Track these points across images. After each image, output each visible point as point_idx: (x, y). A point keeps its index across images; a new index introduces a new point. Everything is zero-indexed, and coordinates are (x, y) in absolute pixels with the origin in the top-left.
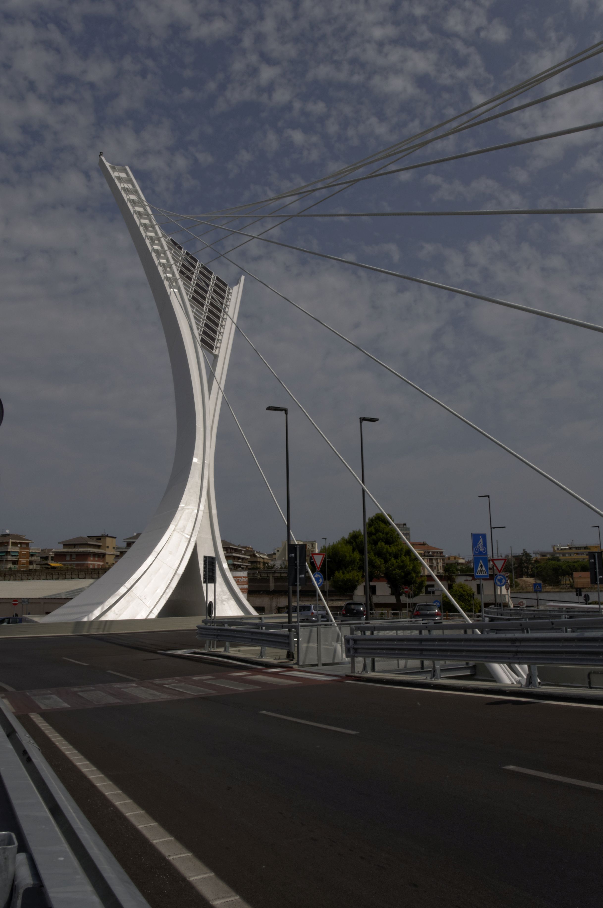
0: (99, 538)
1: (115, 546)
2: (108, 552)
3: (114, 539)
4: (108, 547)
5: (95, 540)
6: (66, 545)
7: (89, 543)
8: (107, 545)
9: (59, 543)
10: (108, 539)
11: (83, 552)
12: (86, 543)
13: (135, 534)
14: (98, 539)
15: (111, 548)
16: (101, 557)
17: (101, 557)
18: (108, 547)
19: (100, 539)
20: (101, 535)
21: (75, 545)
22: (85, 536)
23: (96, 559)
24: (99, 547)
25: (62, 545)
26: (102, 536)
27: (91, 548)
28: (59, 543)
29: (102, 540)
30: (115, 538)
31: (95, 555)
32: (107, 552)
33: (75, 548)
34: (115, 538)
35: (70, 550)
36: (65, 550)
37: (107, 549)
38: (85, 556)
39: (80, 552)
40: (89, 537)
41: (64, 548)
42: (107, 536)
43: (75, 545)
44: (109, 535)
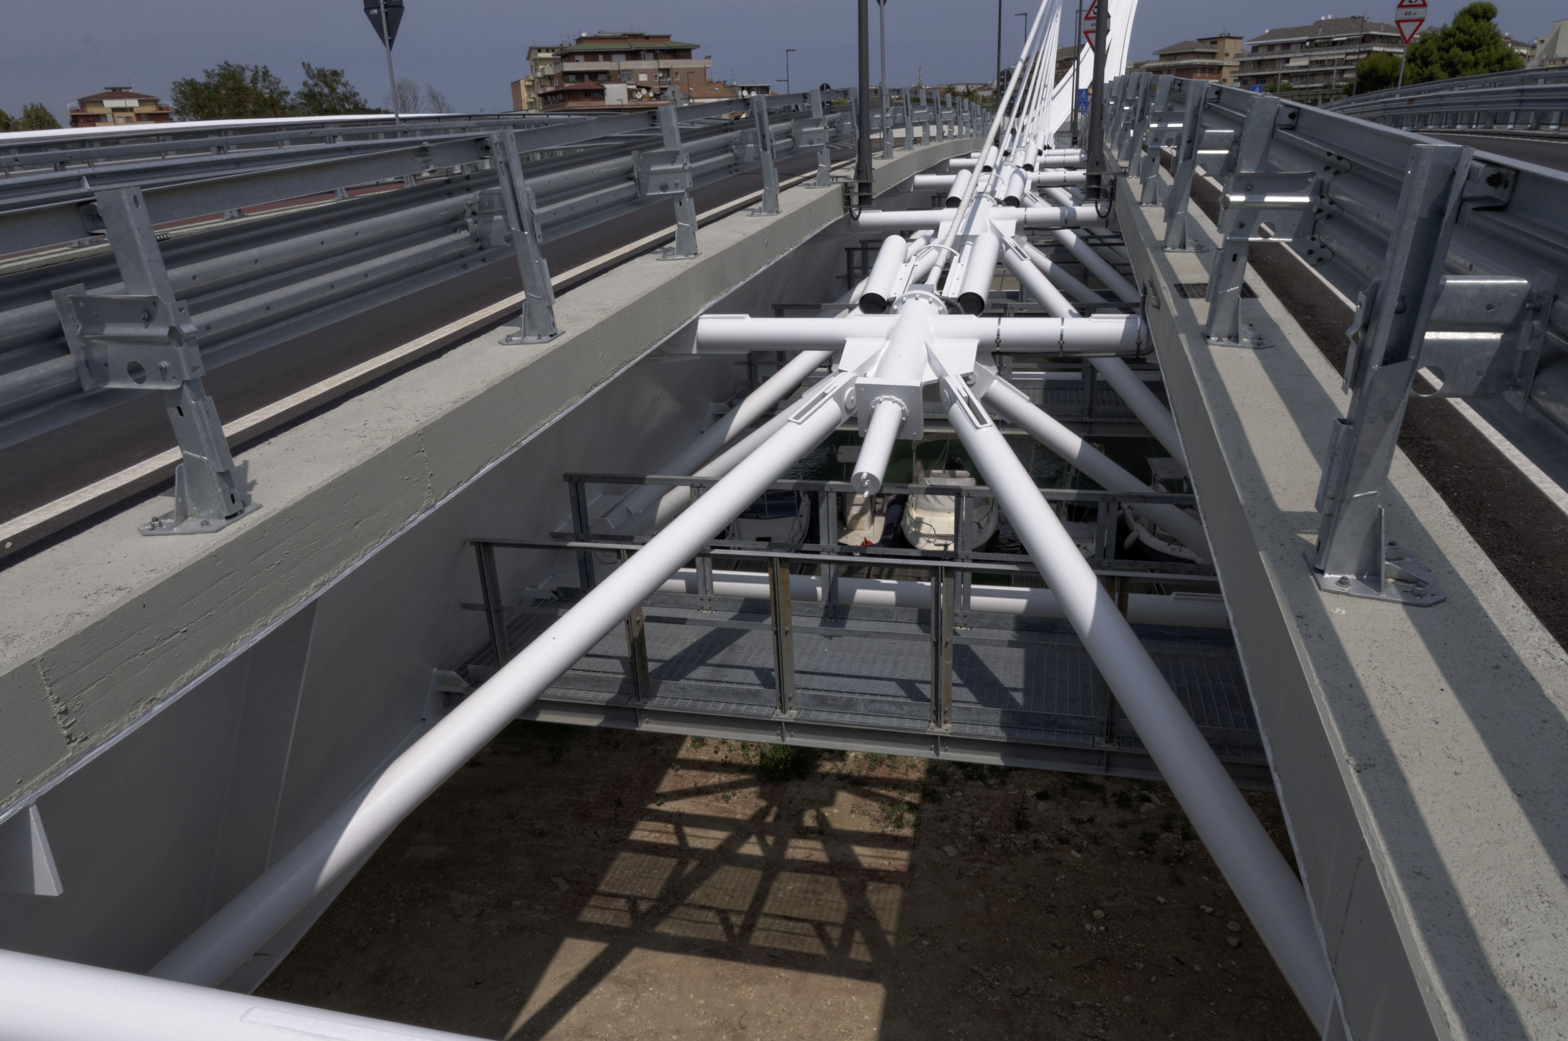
0: (1214, 41)
1: (1239, 52)
2: (1226, 62)
3: (1238, 41)
4: (1227, 55)
5: (1208, 43)
6: (1164, 56)
7: (1196, 50)
8: (1226, 51)
9: (1154, 53)
10: (1227, 41)
11: (1186, 65)
12: (1191, 50)
13: (1267, 31)
14: (1212, 43)
15: (1232, 55)
16: (1216, 71)
17: (1216, 71)
18: (1227, 55)
19: (1216, 43)
20: (1218, 36)
21: (1175, 56)
22: (1193, 37)
23: (1207, 75)
24: (1213, 55)
25: (1157, 57)
26: (1221, 37)
27: (1199, 58)
28: (1154, 53)
29: (1220, 43)
30: (1241, 38)
31: (1204, 68)
32: (1226, 63)
33: (1175, 59)
34: (1241, 38)
35: (1168, 63)
36: (1161, 64)
37: (1226, 58)
38: (1188, 70)
39: (1182, 65)
40: (1199, 40)
41: (1160, 60)
42: (1229, 37)
43: (1175, 56)
44: (1231, 35)
